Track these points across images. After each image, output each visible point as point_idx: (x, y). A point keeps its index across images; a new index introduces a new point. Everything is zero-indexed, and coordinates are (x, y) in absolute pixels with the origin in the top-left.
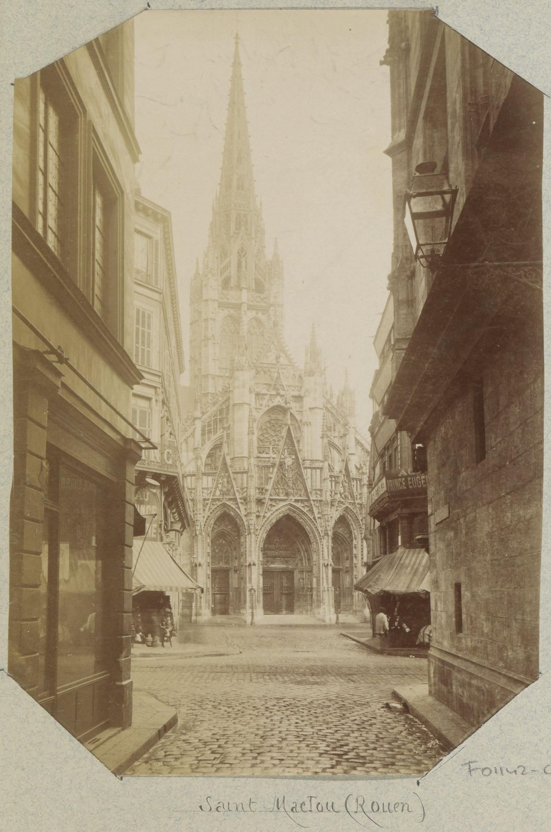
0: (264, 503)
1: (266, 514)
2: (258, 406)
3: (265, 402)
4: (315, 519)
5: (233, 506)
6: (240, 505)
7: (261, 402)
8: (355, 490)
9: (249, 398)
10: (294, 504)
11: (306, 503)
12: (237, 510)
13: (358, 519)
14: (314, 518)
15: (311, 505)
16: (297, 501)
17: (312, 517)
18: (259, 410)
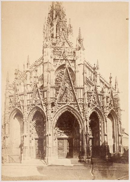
0: (55, 105)
1: (56, 111)
2: (55, 65)
3: (58, 63)
4: (80, 113)
5: (41, 107)
6: (44, 106)
7: (56, 63)
8: (100, 100)
9: (51, 61)
10: (70, 105)
11: (76, 105)
12: (42, 109)
13: (102, 114)
14: (80, 112)
15: (78, 106)
16: (71, 104)
17: (79, 112)
18: (55, 67)
